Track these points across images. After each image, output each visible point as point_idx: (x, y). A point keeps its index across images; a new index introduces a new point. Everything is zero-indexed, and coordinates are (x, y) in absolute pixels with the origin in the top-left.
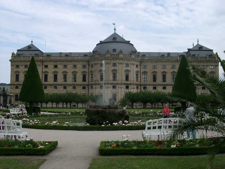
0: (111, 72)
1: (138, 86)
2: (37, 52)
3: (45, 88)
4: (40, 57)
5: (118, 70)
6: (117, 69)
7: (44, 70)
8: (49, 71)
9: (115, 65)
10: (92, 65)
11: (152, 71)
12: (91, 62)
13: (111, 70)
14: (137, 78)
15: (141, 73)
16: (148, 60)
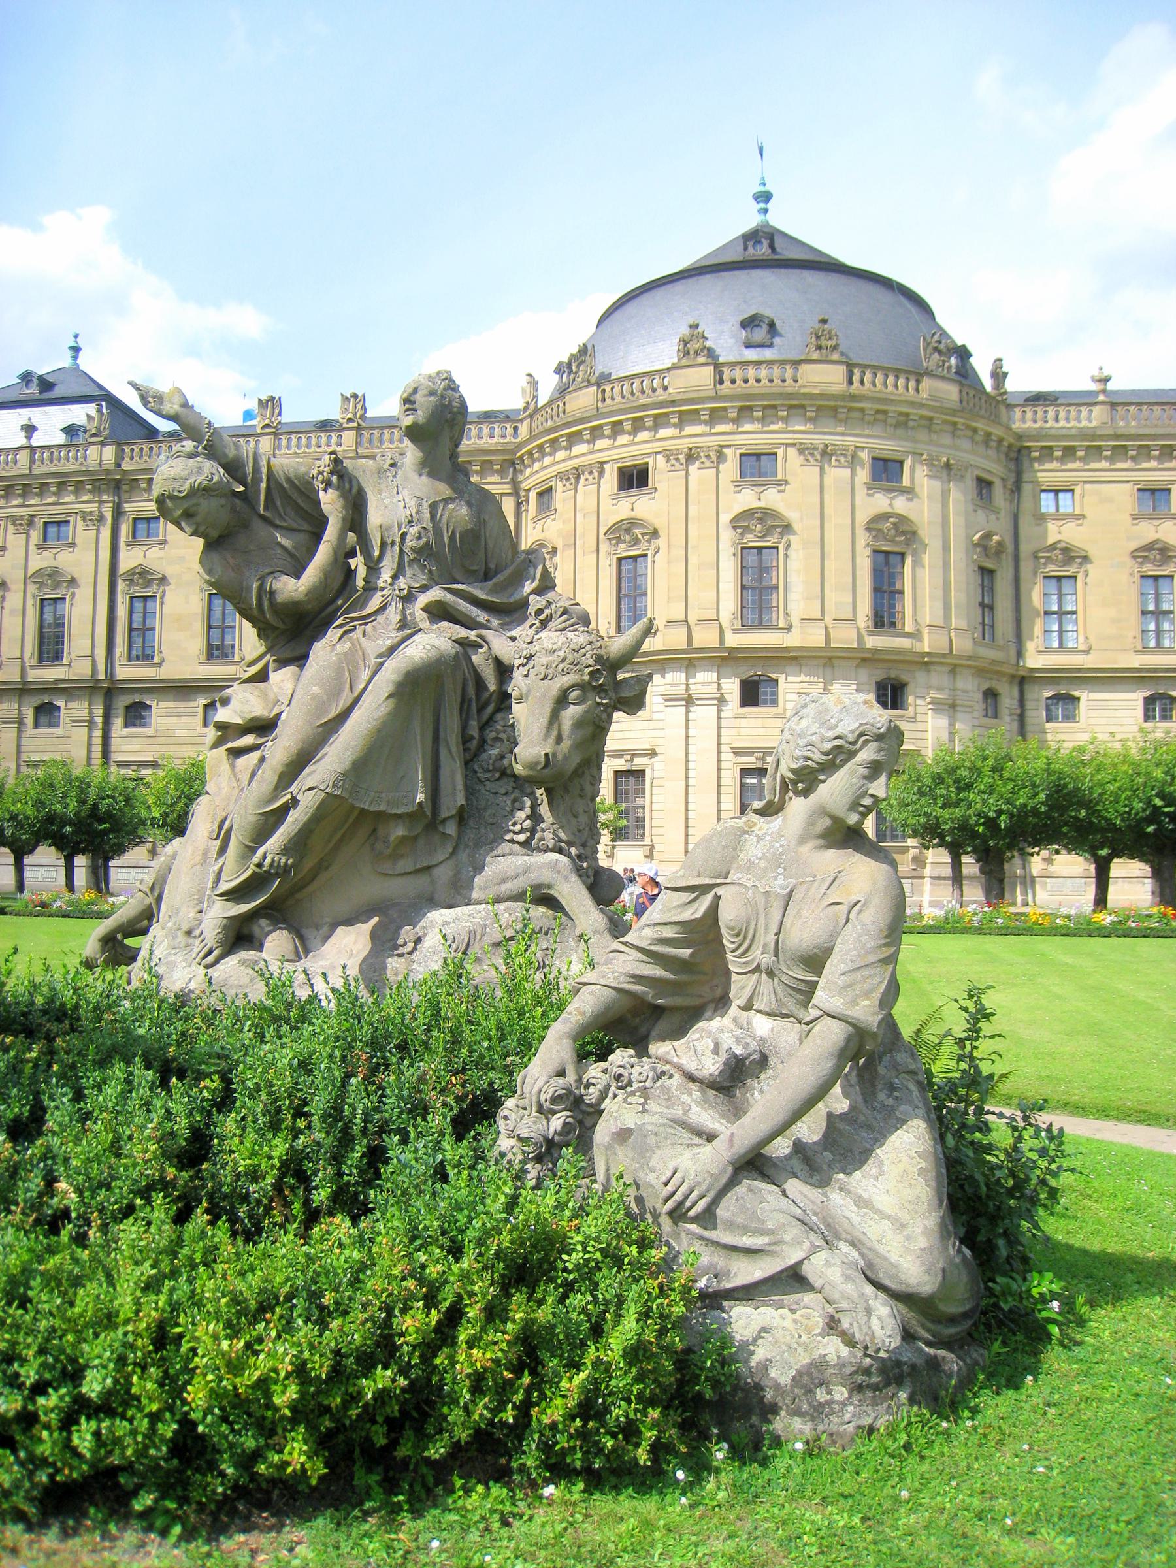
0: (727, 535)
1: (994, 684)
2: (79, 414)
3: (136, 714)
4: (93, 452)
5: (791, 515)
6: (781, 508)
7: (129, 560)
8: (169, 571)
9: (757, 466)
10: (545, 494)
11: (1135, 545)
12: (537, 466)
13: (725, 518)
14: (987, 607)
15: (1022, 564)
16: (1084, 435)
